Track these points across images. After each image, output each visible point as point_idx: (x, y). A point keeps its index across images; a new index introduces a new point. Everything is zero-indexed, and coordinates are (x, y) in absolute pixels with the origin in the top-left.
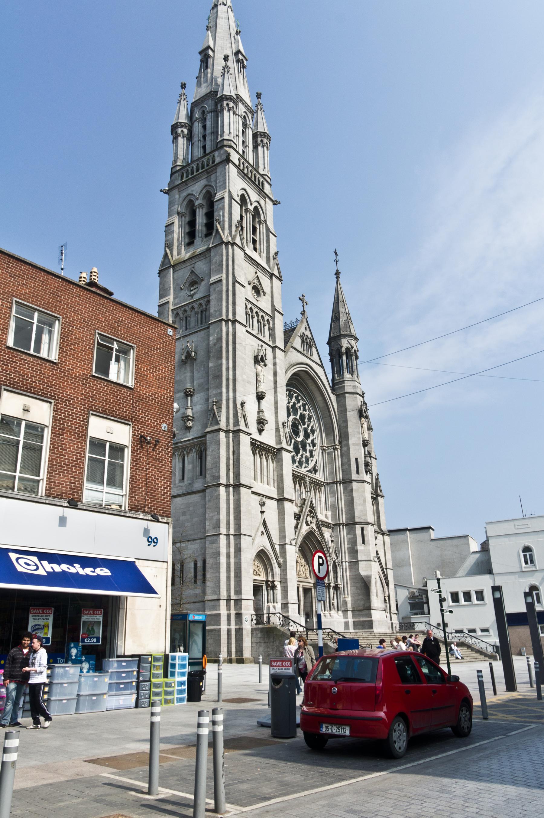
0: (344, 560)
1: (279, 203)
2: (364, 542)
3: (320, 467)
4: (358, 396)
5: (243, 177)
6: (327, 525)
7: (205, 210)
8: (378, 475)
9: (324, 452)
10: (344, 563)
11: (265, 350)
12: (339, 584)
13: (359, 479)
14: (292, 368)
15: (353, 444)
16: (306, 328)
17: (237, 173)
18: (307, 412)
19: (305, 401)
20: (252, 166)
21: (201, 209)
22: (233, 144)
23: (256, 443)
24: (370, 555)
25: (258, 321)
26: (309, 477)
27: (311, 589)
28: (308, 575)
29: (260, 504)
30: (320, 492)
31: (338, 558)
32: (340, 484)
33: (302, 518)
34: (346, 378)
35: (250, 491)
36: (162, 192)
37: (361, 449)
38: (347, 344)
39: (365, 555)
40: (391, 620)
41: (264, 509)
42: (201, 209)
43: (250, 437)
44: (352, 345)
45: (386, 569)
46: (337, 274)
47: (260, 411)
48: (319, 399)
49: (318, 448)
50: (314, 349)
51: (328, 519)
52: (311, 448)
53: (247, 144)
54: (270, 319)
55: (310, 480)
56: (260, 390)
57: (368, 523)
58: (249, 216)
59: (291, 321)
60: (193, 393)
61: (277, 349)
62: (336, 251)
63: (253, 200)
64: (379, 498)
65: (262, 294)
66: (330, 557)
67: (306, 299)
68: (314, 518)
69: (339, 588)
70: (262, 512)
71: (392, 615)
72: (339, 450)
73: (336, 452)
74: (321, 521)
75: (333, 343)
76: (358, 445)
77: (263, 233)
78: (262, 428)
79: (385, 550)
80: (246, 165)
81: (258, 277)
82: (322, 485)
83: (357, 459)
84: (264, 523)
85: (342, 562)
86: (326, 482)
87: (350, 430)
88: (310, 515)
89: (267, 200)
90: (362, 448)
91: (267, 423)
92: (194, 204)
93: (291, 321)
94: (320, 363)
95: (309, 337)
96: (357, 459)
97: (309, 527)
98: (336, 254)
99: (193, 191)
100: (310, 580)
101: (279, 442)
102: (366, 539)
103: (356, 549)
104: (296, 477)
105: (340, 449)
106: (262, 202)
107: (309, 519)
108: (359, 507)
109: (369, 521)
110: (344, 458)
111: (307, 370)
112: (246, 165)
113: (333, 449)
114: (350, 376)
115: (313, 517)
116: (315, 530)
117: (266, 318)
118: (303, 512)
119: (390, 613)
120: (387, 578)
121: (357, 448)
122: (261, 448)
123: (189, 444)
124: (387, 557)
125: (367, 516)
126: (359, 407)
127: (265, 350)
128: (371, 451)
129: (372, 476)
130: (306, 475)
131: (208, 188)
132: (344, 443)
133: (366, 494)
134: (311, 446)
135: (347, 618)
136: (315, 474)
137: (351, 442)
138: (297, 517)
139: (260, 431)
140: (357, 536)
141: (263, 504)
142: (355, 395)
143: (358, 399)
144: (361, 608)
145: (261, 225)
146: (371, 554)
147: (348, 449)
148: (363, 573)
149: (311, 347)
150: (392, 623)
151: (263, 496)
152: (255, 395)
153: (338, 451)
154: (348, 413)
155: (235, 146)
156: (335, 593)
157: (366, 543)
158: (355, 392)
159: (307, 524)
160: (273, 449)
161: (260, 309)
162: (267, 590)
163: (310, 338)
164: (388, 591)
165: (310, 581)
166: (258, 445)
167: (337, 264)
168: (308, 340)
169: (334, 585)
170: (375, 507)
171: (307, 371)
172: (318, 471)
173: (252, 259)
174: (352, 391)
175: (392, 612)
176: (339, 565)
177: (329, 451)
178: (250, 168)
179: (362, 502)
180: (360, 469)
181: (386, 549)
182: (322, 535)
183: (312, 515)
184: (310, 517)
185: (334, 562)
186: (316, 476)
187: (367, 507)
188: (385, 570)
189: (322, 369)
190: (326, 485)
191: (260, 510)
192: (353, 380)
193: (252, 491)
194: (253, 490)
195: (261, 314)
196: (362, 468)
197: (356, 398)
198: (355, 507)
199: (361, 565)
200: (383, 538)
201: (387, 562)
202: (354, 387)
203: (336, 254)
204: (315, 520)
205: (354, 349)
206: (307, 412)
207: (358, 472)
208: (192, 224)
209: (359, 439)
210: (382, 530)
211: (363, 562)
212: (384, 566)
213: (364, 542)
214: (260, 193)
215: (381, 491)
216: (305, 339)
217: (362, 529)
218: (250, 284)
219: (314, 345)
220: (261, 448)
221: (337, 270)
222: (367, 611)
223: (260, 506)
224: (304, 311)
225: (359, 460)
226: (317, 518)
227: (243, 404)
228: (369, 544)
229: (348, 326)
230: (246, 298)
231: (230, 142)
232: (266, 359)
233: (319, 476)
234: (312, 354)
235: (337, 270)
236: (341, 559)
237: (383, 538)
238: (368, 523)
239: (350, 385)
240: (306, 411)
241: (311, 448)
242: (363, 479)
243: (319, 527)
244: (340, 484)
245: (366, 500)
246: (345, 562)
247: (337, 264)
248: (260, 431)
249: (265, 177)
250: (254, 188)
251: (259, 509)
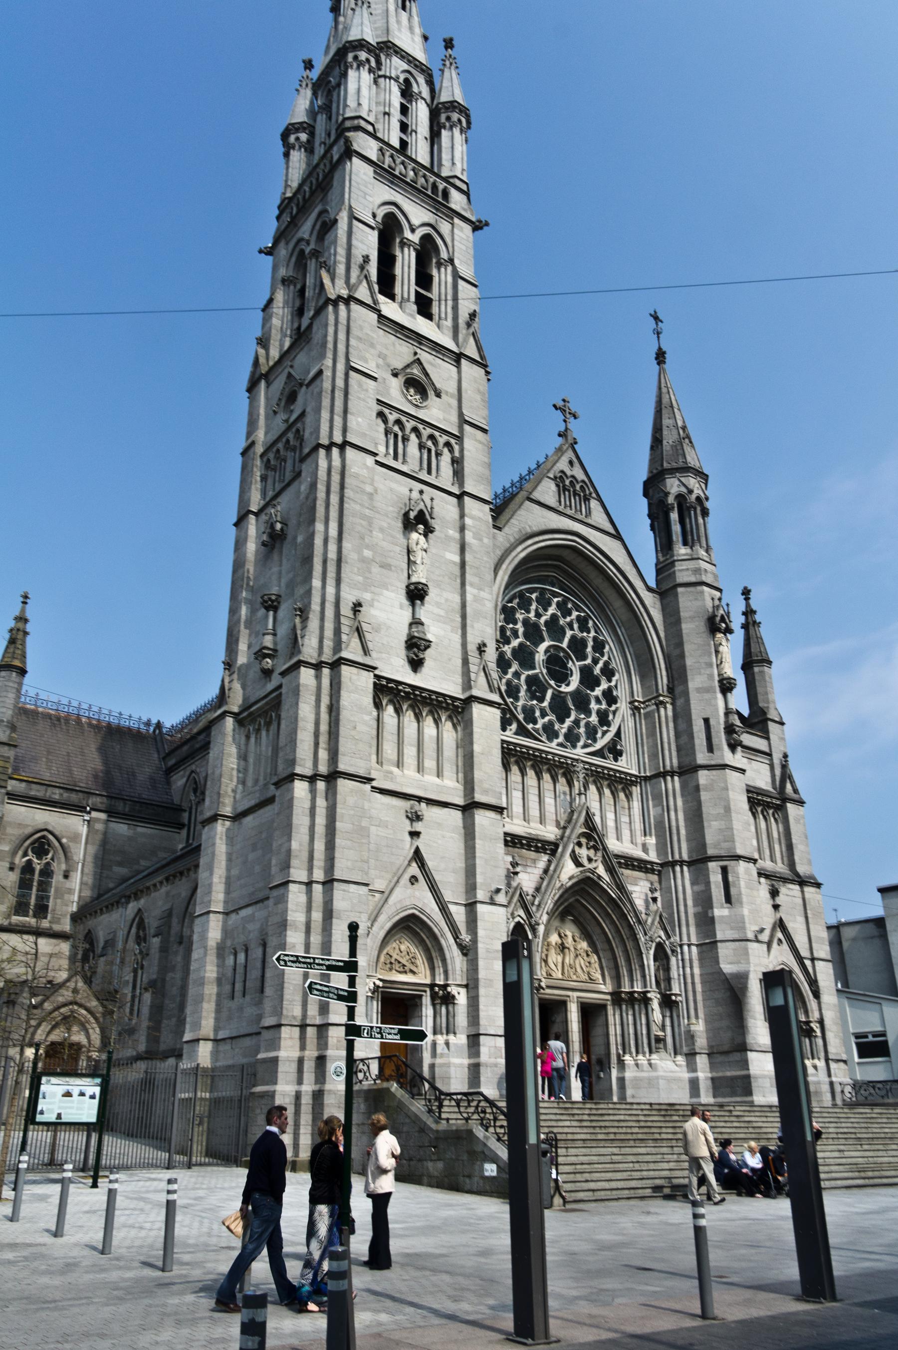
0: (685, 940)
1: (487, 224)
2: (728, 899)
3: (628, 743)
4: (706, 589)
5: (392, 183)
6: (642, 866)
8: (785, 756)
9: (637, 714)
10: (686, 948)
11: (432, 499)
12: (676, 995)
13: (713, 763)
14: (530, 542)
15: (699, 690)
16: (571, 463)
18: (593, 634)
19: (585, 612)
22: (363, 123)
23: (400, 688)
24: (743, 928)
25: (421, 446)
26: (583, 761)
27: (602, 1007)
28: (598, 976)
29: (407, 817)
30: (629, 796)
31: (669, 937)
32: (672, 777)
33: (560, 850)
34: (679, 555)
35: (368, 787)
36: (263, 255)
37: (716, 698)
38: (678, 486)
39: (732, 929)
40: (829, 1075)
41: (418, 826)
43: (372, 674)
44: (691, 487)
45: (813, 960)
46: (660, 357)
47: (416, 622)
48: (618, 603)
49: (623, 706)
50: (594, 504)
51: (647, 853)
52: (604, 706)
54: (453, 441)
55: (586, 769)
56: (414, 579)
57: (738, 858)
60: (279, 603)
61: (466, 498)
62: (655, 312)
63: (416, 222)
64: (789, 805)
65: (431, 393)
66: (646, 934)
67: (573, 406)
68: (598, 850)
69: (676, 1002)
70: (415, 834)
71: (833, 1065)
72: (669, 707)
73: (662, 711)
74: (617, 856)
75: (651, 491)
76: (709, 690)
77: (446, 283)
78: (417, 656)
79: (807, 918)
81: (418, 362)
82: (633, 783)
83: (706, 721)
84: (417, 856)
85: (681, 946)
86: (643, 774)
87: (689, 662)
88: (587, 844)
89: (456, 221)
90: (720, 696)
91: (429, 647)
94: (612, 531)
95: (579, 479)
96: (706, 721)
97: (581, 869)
98: (656, 318)
100: (603, 986)
101: (467, 684)
102: (733, 891)
103: (710, 915)
104: (557, 766)
105: (672, 704)
106: (445, 227)
107: (583, 852)
108: (714, 823)
109: (740, 852)
110: (680, 721)
111: (558, 540)
113: (657, 705)
114: (689, 551)
115: (596, 849)
116: (599, 877)
117: (442, 439)
118: (565, 839)
119: (827, 1060)
120: (816, 981)
121: (707, 696)
122: (415, 700)
123: (267, 704)
124: (812, 934)
125: (733, 841)
126: (711, 610)
127: (432, 499)
128: (768, 707)
129: (771, 760)
130: (577, 760)
132: (679, 689)
133: (730, 793)
134: (604, 702)
135: (694, 1070)
136: (616, 760)
137: (691, 685)
138: (551, 850)
139: (416, 664)
140: (713, 886)
141: (415, 817)
142: (699, 588)
143: (706, 594)
144: (726, 1048)
145: (443, 270)
146: (747, 925)
147: (688, 701)
148: (727, 968)
149: (587, 499)
150: (831, 1084)
151: (420, 799)
152: (403, 592)
153: (665, 708)
154: (684, 626)
156: (668, 1014)
157: (733, 900)
158: (698, 580)
159: (578, 864)
160: (450, 702)
161: (423, 422)
162: (434, 1005)
163: (583, 481)
164: (820, 1010)
165: (602, 988)
166: (405, 692)
167: (658, 337)
168: (578, 487)
169: (659, 996)
170: (781, 826)
171: (575, 547)
172: (624, 755)
173: (402, 327)
174: (693, 579)
175: (831, 1057)
176: (673, 951)
177: (648, 709)
179: (722, 811)
180: (715, 741)
181: (809, 915)
182: (621, 887)
183: (592, 843)
184: (588, 849)
185: (660, 947)
186: (619, 763)
187: (734, 822)
188: (808, 963)
189: (617, 544)
190: (643, 783)
191: (409, 829)
192: (695, 556)
193: (372, 787)
194: (374, 784)
195: (426, 432)
196: (720, 738)
197: (702, 592)
198: (706, 824)
199: (724, 951)
200: (803, 892)
201: (814, 945)
202: (697, 571)
203: (656, 318)
204: (600, 854)
205: (694, 496)
206: (593, 634)
207: (710, 749)
209: (711, 676)
210: (797, 875)
211: (727, 944)
212: (804, 952)
213: (728, 899)
214: (437, 210)
215: (796, 791)
216: (578, 487)
217: (724, 871)
218: (395, 375)
219: (594, 495)
220: (415, 700)
221: (660, 349)
222: (738, 1054)
223: (408, 822)
224: (566, 429)
225: (712, 722)
226: (605, 849)
227: (357, 607)
228: (741, 903)
229: (681, 452)
230: (378, 400)
231: (356, 122)
232: (432, 518)
233: (628, 764)
234: (589, 513)
235: (660, 349)
236: (678, 938)
237: (803, 892)
238: (738, 858)
239: (688, 569)
240: (589, 632)
241: (604, 706)
242: (721, 762)
243: (610, 870)
244: (672, 777)
245: (732, 807)
246: (689, 945)
247: (658, 337)
248: (416, 664)
249: (451, 180)
250: (422, 201)
251: (407, 826)
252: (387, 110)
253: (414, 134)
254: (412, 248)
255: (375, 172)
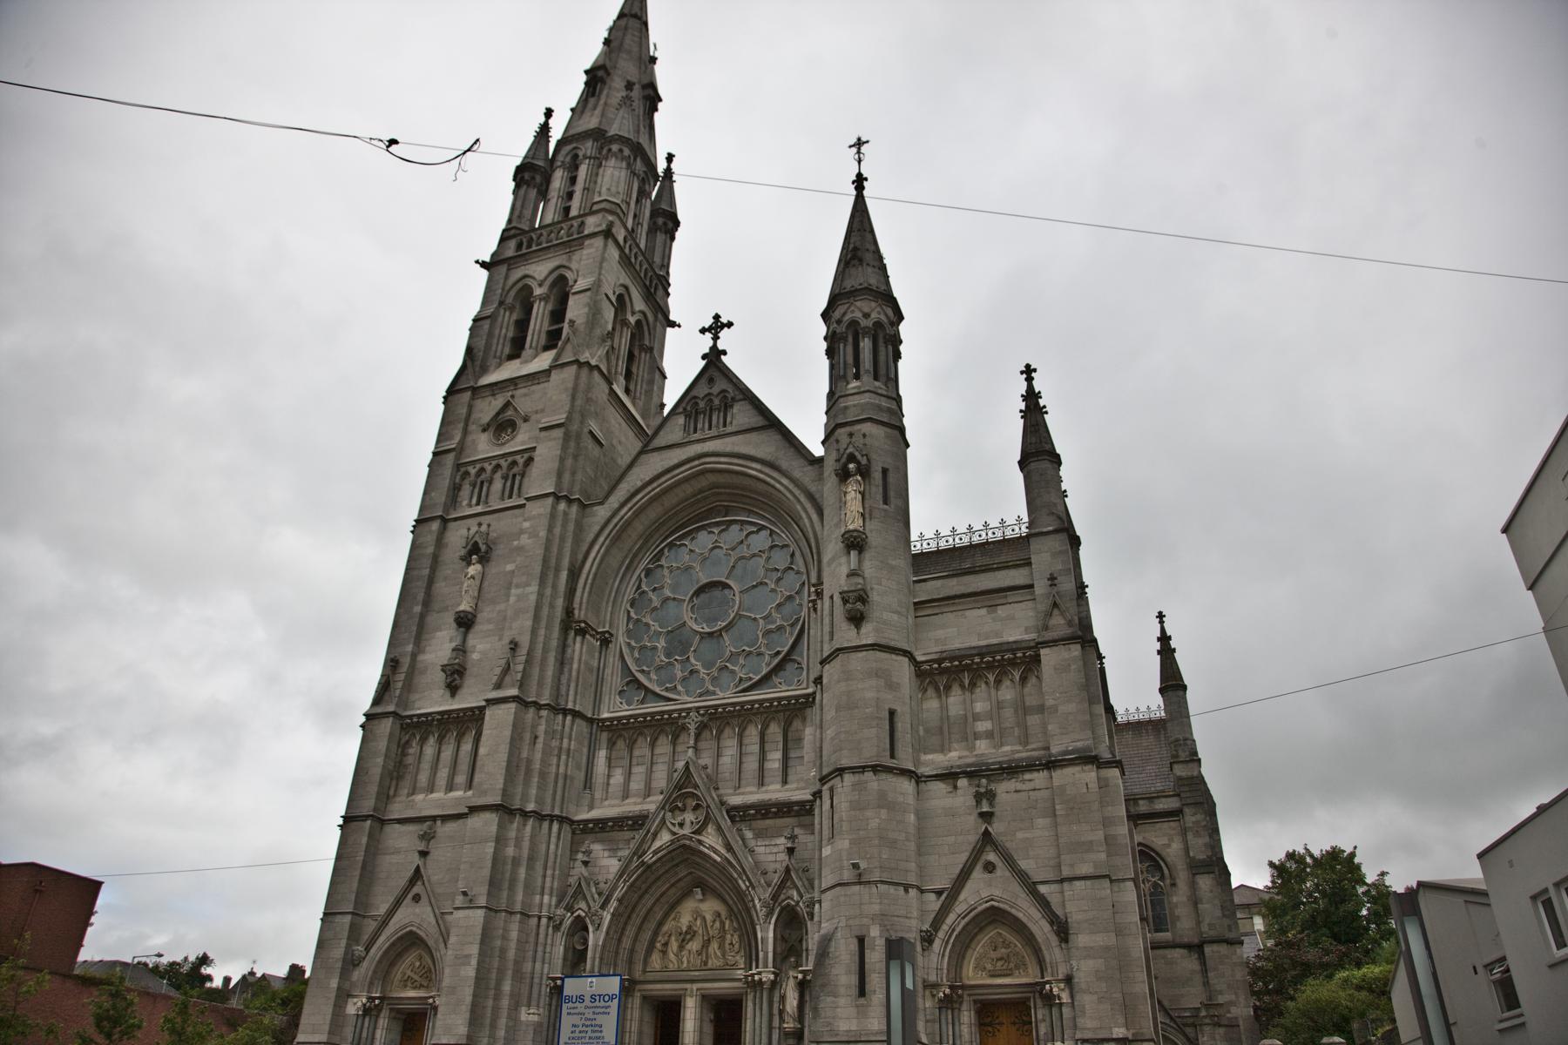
7: (550, 307)
17: (617, 257)
20: (643, 254)
21: (542, 303)
42: (542, 303)
53: (641, 221)
58: (627, 335)
59: (937, 533)
80: (635, 250)
92: (532, 293)
93: (937, 533)
99: (535, 271)
112: (635, 250)
131: (562, 271)
155: (621, 215)
178: (640, 258)
208: (522, 325)
252: (628, 200)
253: (640, 226)
254: (630, 330)
255: (620, 257)
